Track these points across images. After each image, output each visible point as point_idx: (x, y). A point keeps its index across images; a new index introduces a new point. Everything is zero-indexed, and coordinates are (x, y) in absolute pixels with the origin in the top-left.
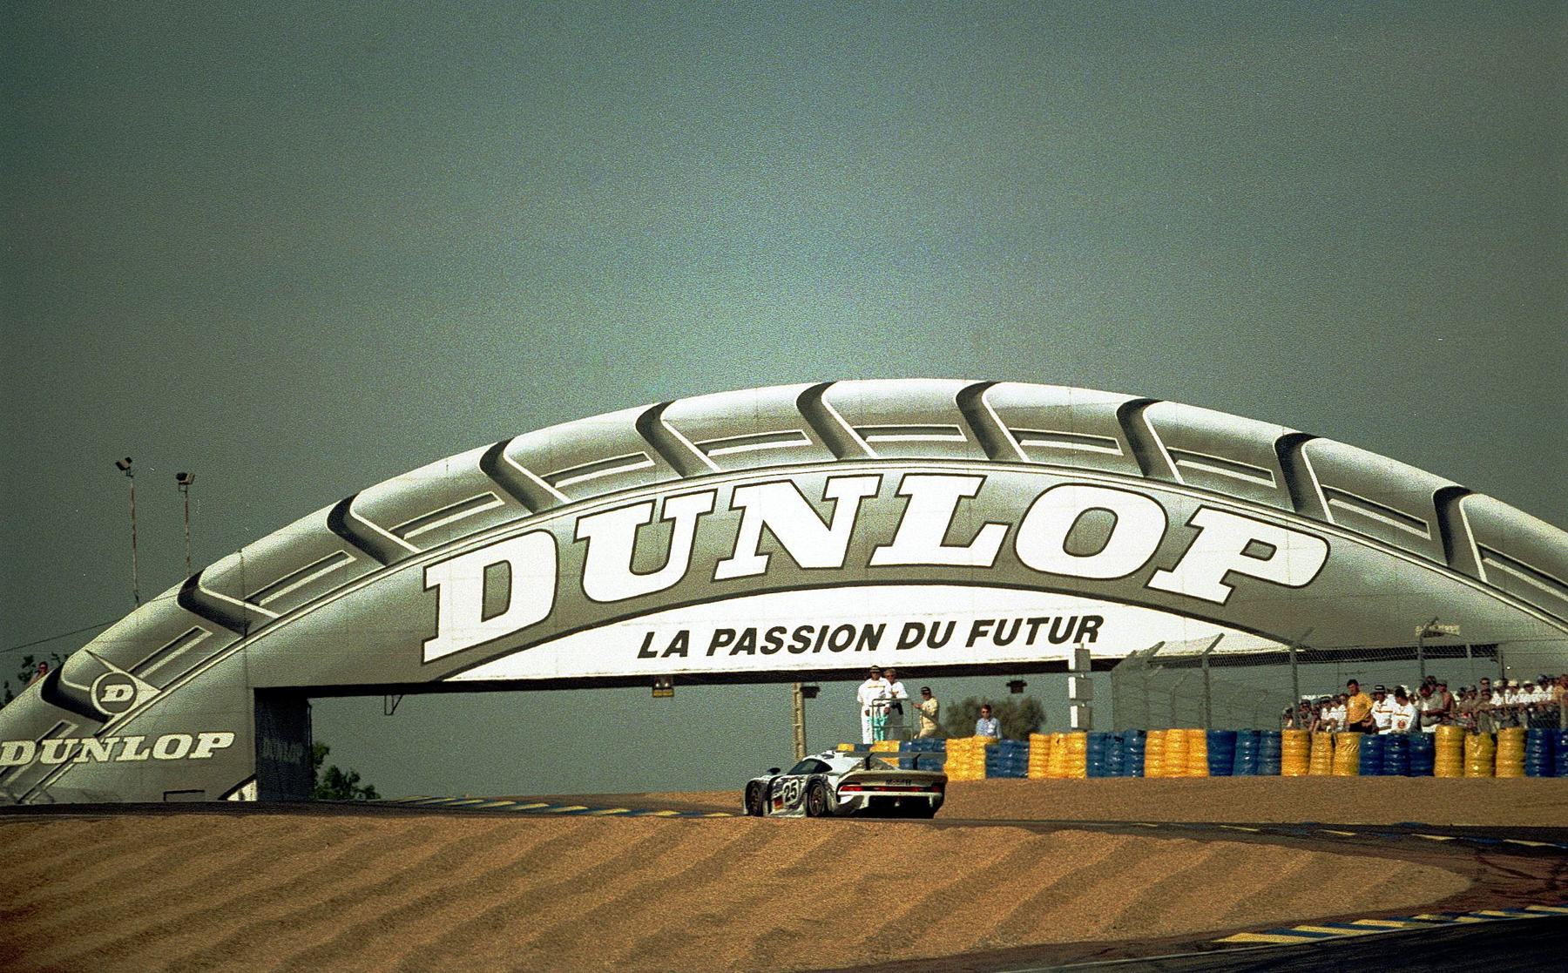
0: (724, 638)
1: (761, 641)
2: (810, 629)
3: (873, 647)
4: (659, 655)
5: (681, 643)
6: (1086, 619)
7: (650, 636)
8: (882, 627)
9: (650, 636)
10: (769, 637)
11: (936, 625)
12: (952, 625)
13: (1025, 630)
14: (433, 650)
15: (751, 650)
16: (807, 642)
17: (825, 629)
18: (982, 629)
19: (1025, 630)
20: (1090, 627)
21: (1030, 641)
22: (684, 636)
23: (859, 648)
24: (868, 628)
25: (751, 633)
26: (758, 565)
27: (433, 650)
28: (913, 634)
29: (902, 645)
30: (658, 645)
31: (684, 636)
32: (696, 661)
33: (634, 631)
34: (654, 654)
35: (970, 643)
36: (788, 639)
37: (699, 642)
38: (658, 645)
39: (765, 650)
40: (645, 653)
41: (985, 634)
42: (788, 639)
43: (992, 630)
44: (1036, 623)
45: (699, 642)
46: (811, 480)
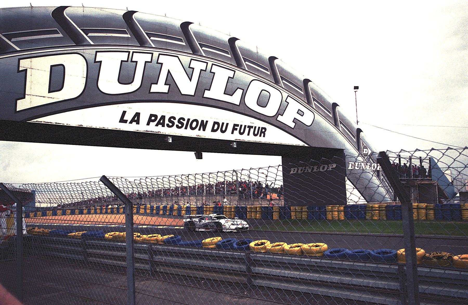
0: (153, 118)
1: (167, 122)
2: (184, 119)
3: (204, 130)
4: (128, 122)
5: (136, 118)
6: (262, 128)
7: (124, 113)
8: (207, 122)
9: (124, 113)
10: (170, 120)
11: (223, 124)
12: (227, 124)
13: (247, 129)
14: (22, 105)
15: (163, 126)
16: (183, 124)
17: (189, 120)
18: (236, 127)
19: (247, 129)
20: (263, 132)
21: (248, 134)
22: (138, 115)
23: (199, 130)
24: (202, 121)
25: (163, 117)
26: (165, 89)
27: (22, 105)
28: (216, 126)
29: (213, 130)
30: (128, 117)
31: (138, 115)
32: (142, 127)
33: (117, 109)
34: (126, 122)
35: (232, 133)
36: (176, 122)
37: (144, 119)
38: (128, 117)
39: (168, 126)
40: (122, 120)
41: (236, 129)
42: (176, 122)
43: (238, 128)
44: (250, 127)
45: (144, 119)
46: (186, 59)
